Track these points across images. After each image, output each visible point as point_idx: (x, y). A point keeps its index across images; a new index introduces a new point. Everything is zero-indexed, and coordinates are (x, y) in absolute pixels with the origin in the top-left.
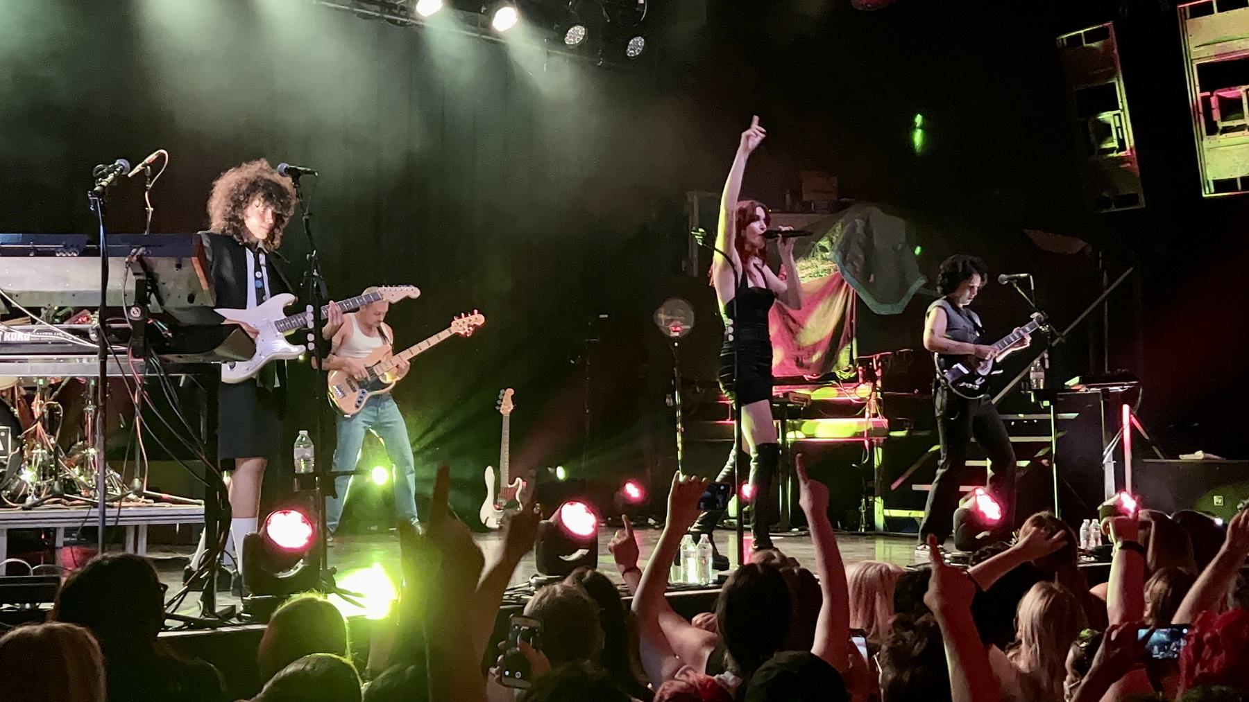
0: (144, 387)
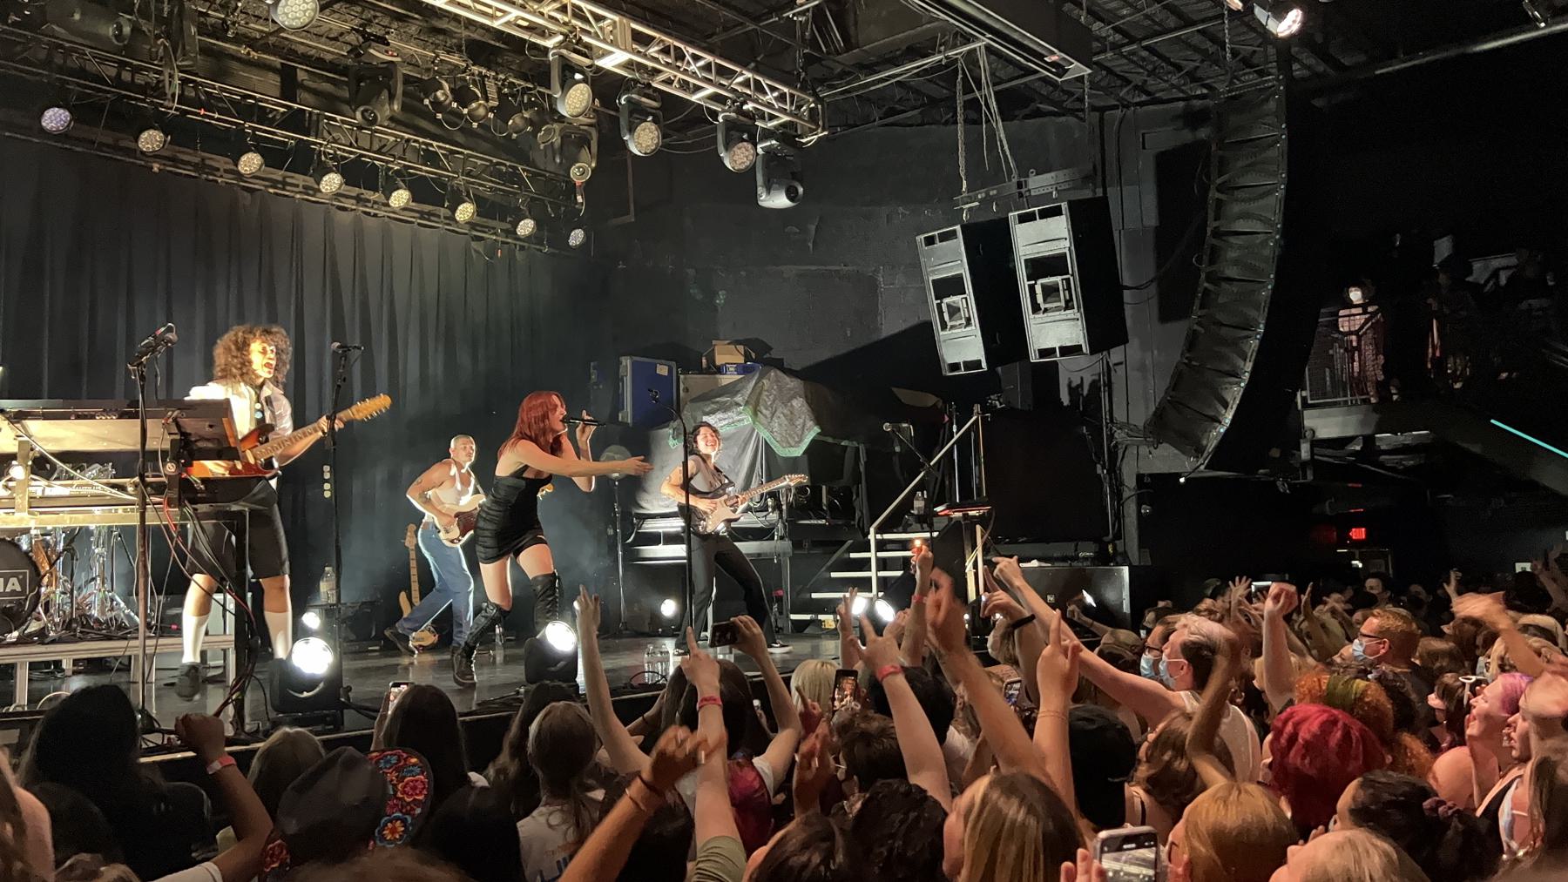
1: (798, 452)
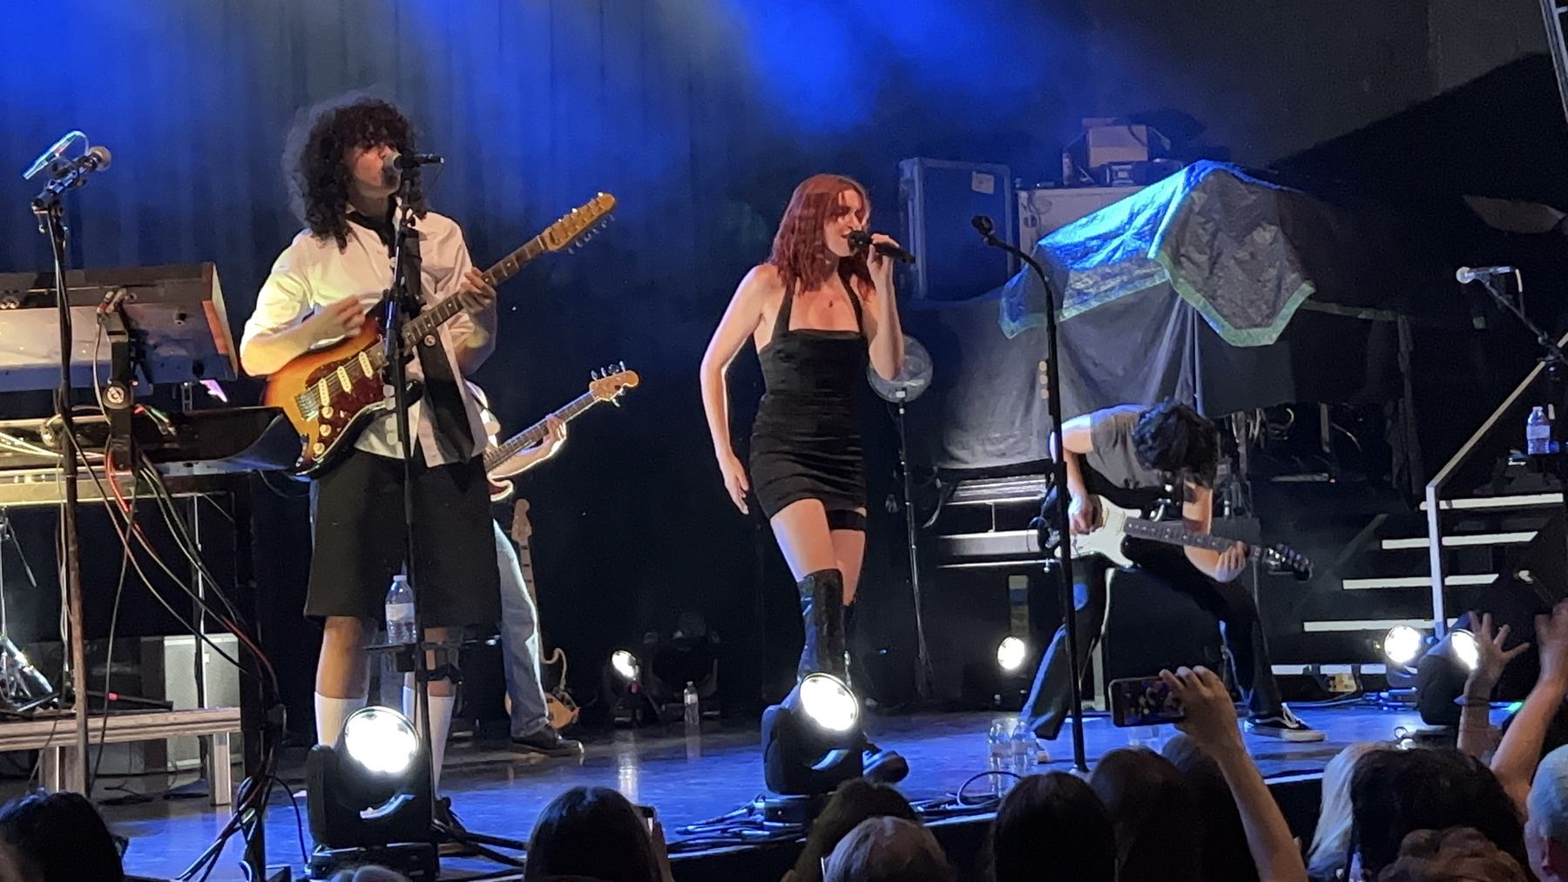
0: (136, 518)
1: (1268, 336)
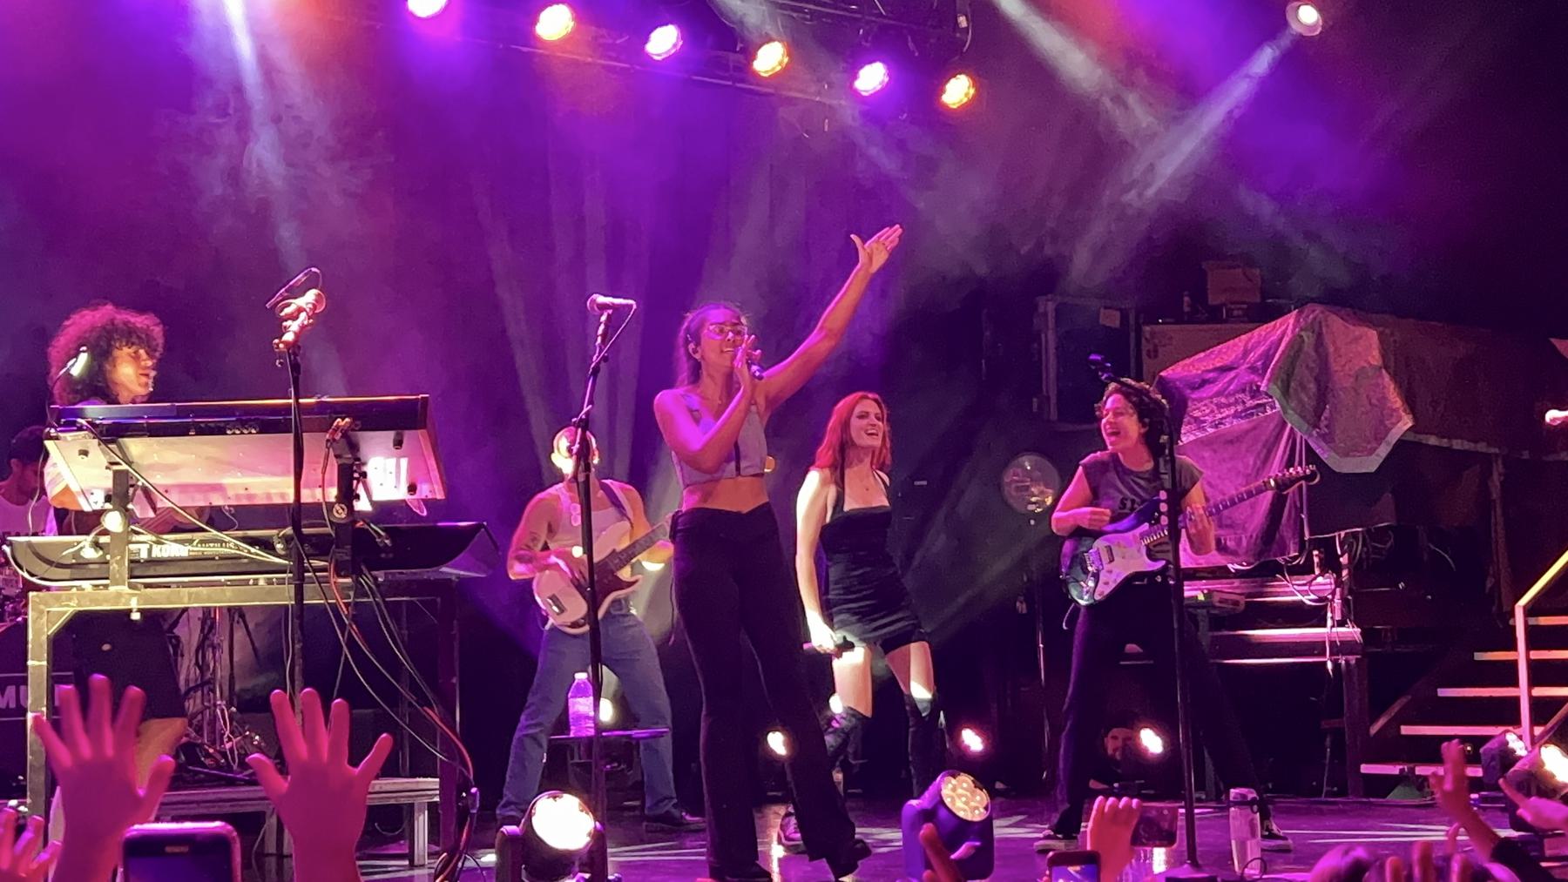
0: (354, 619)
1: (1370, 464)
